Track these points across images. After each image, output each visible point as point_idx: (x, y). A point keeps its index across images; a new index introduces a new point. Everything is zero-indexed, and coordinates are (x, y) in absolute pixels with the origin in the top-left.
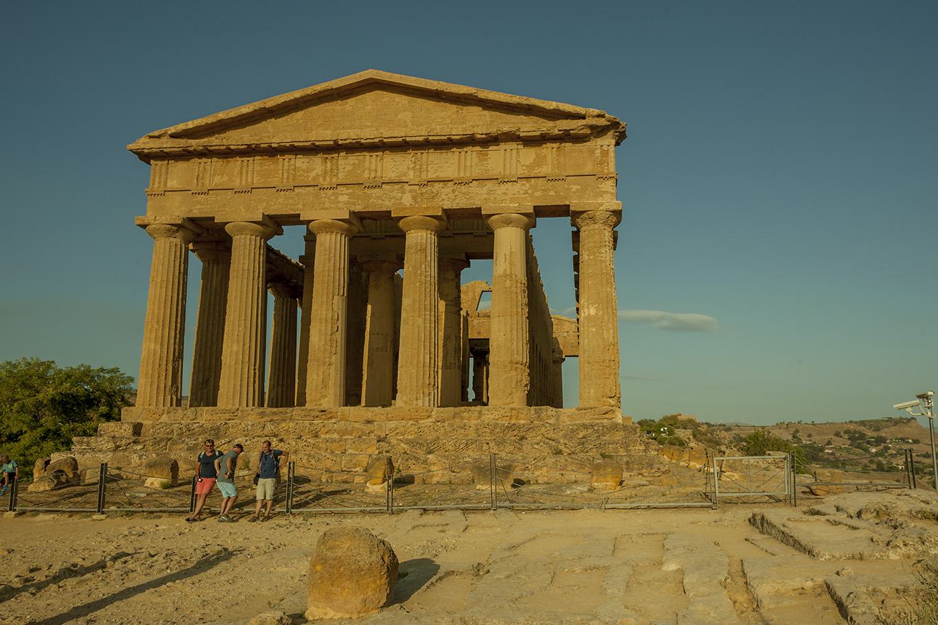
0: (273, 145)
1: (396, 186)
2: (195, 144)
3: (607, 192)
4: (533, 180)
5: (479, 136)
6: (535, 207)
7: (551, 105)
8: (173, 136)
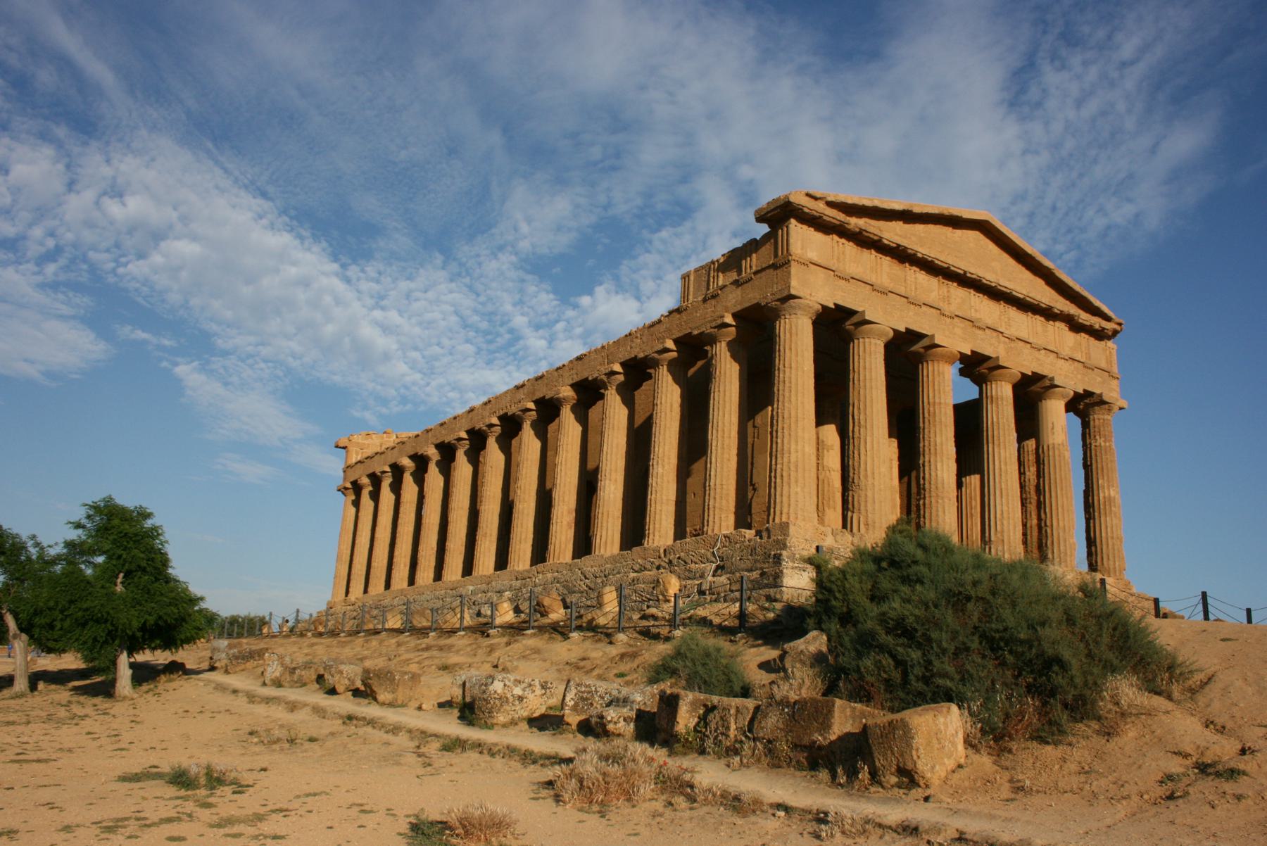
0: (919, 255)
1: (995, 334)
2: (855, 223)
3: (1115, 390)
4: (1076, 363)
5: (1056, 311)
6: (1084, 390)
7: (1097, 303)
8: (831, 204)
